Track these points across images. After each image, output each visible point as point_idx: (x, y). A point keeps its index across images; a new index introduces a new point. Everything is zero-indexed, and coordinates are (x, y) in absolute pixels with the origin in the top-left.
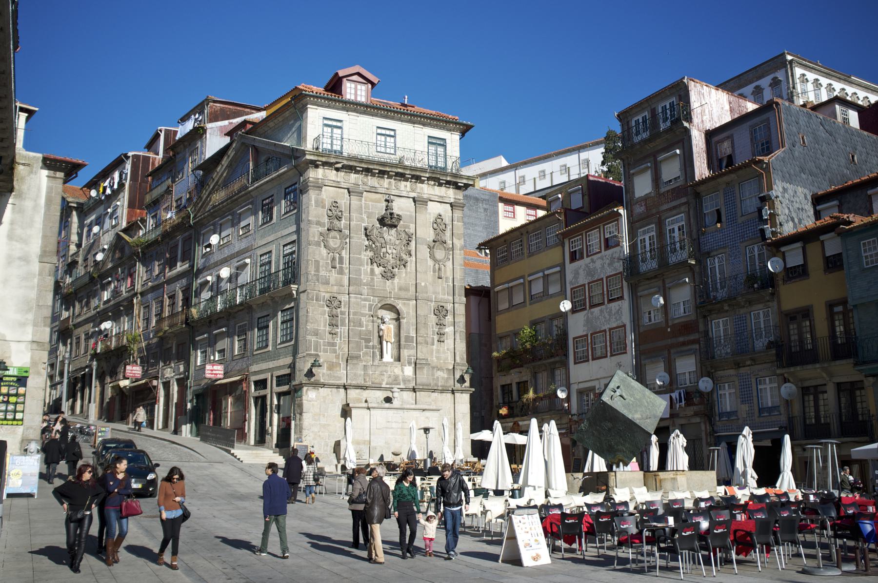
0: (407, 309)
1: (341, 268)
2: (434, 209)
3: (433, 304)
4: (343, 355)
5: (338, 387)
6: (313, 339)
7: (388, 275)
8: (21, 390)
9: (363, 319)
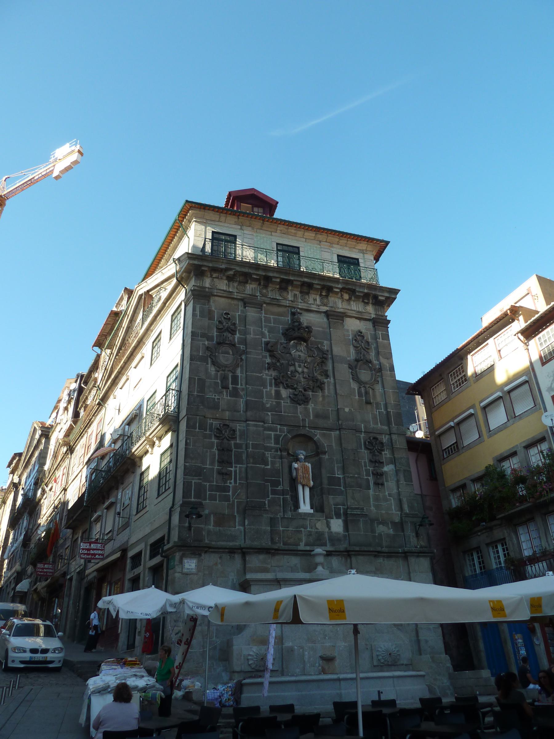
0: (328, 440)
2: (353, 325)
3: (363, 435)
5: (232, 551)
6: (194, 481)
7: (299, 399)
9: (268, 454)
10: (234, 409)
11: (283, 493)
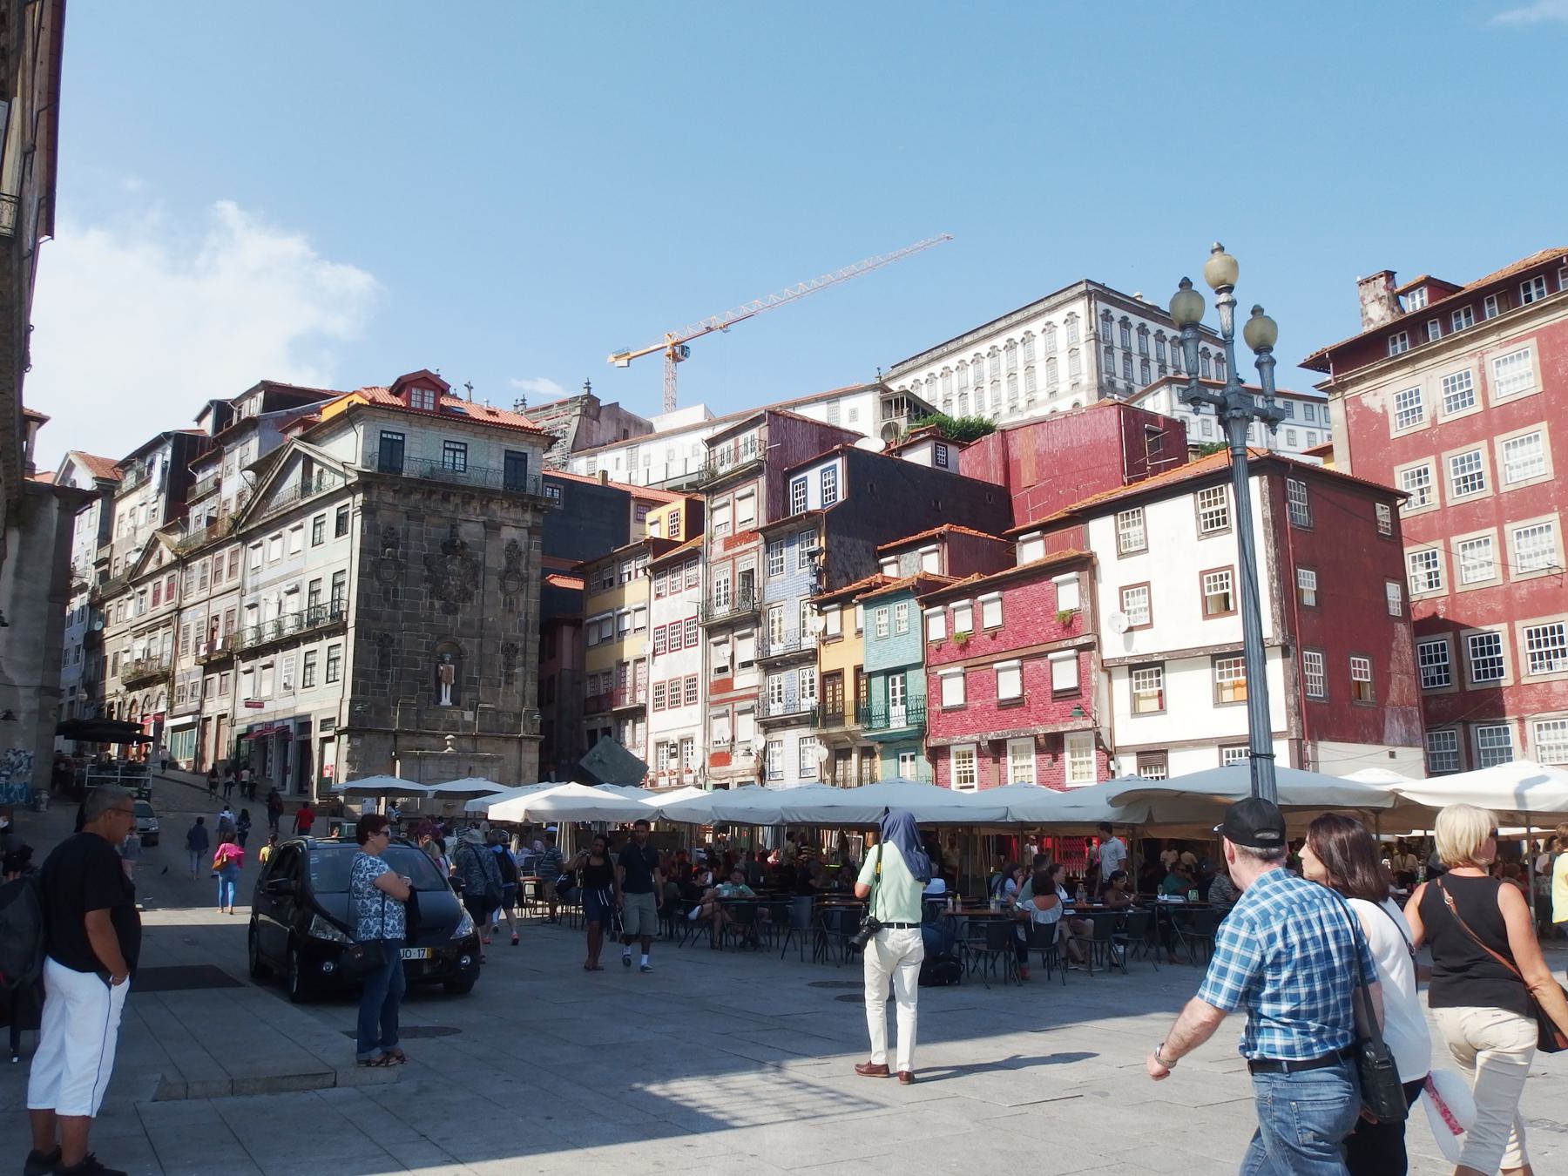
0: (470, 646)
2: (509, 533)
7: (450, 610)
11: (429, 690)
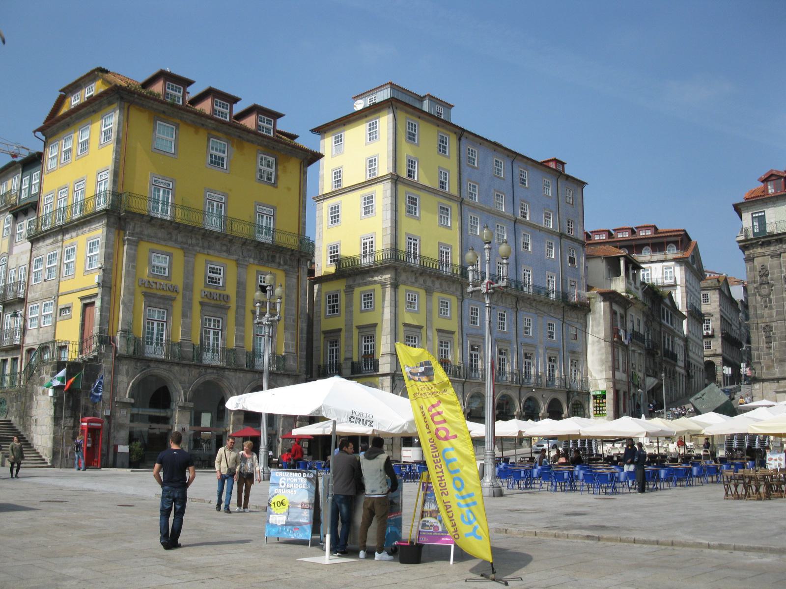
1: (771, 306)
4: (776, 359)
5: (773, 380)
8: (604, 400)
10: (771, 316)
